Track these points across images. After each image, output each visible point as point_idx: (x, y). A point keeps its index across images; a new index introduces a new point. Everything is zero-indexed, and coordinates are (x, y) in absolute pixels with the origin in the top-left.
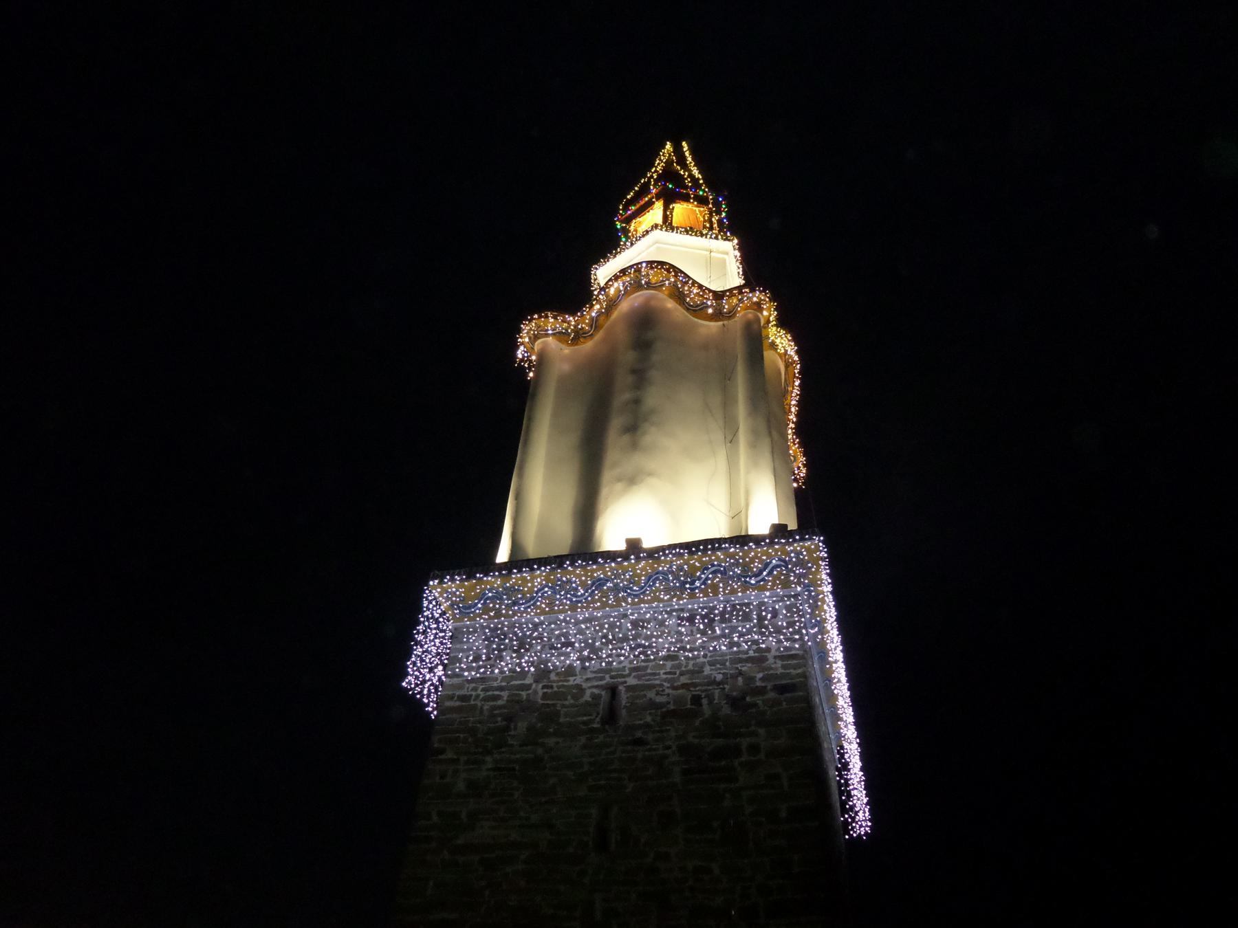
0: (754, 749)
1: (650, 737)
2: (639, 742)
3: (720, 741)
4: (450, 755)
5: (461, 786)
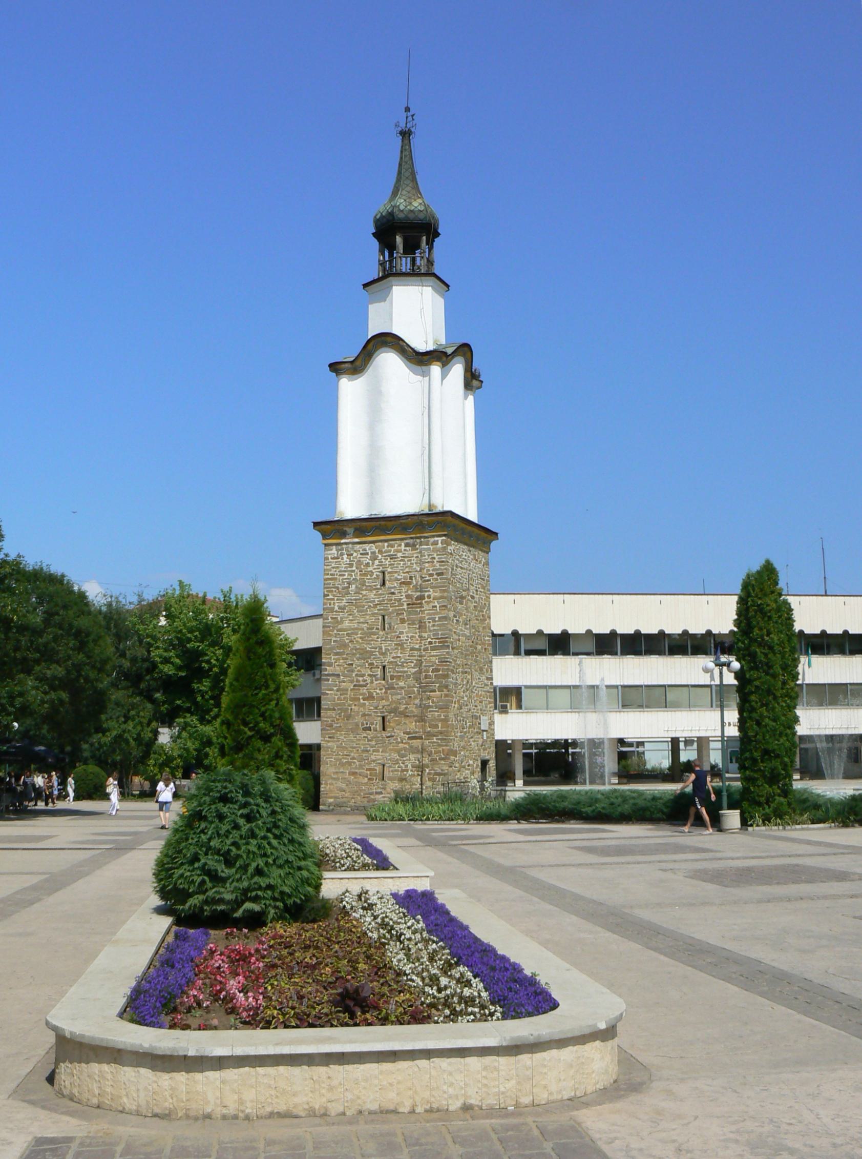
0: (429, 597)
1: (396, 592)
2: (393, 593)
3: (419, 594)
4: (331, 597)
5: (336, 608)
